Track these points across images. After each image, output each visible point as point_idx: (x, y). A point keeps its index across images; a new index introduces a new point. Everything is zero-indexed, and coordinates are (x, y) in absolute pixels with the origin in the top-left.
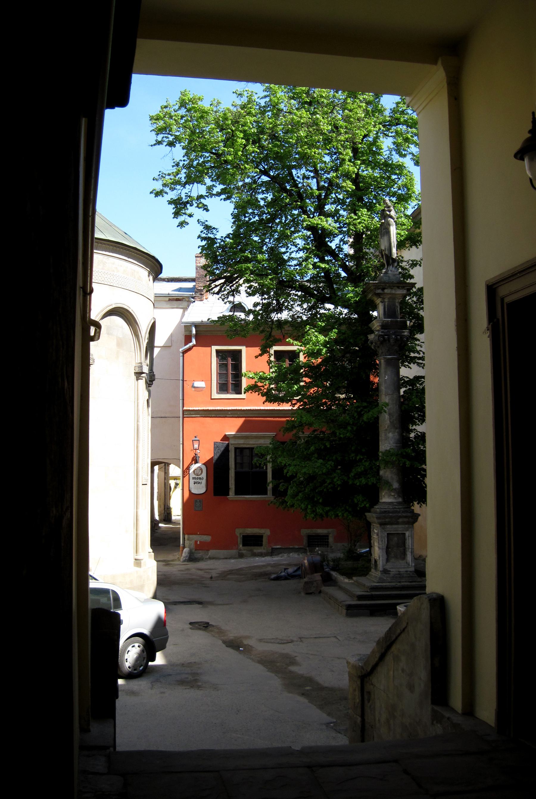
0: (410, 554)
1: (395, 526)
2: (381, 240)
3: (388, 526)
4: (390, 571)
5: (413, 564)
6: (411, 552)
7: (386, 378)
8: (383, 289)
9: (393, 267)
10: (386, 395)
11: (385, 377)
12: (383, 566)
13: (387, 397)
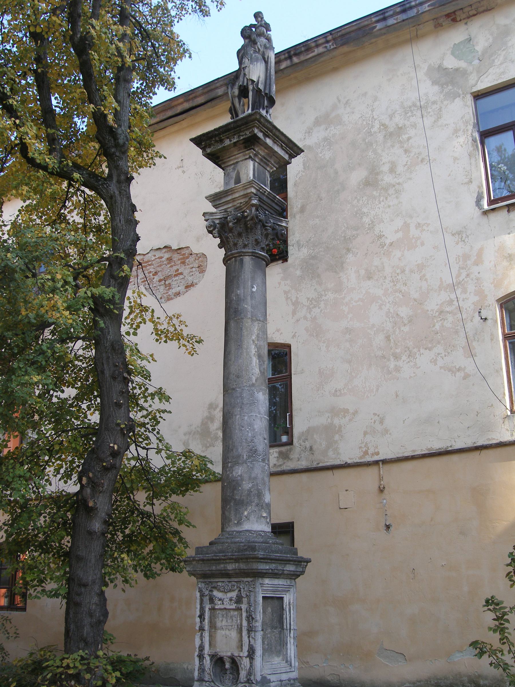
0: (292, 641)
1: (276, 582)
2: (251, 66)
3: (267, 581)
4: (269, 681)
5: (297, 664)
6: (294, 638)
7: (254, 290)
8: (266, 135)
9: (267, 112)
10: (252, 320)
11: (253, 287)
12: (261, 671)
13: (256, 324)
